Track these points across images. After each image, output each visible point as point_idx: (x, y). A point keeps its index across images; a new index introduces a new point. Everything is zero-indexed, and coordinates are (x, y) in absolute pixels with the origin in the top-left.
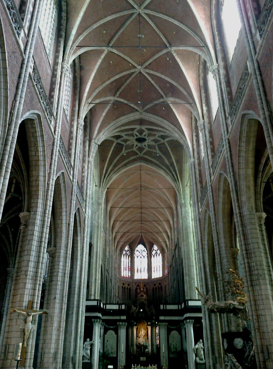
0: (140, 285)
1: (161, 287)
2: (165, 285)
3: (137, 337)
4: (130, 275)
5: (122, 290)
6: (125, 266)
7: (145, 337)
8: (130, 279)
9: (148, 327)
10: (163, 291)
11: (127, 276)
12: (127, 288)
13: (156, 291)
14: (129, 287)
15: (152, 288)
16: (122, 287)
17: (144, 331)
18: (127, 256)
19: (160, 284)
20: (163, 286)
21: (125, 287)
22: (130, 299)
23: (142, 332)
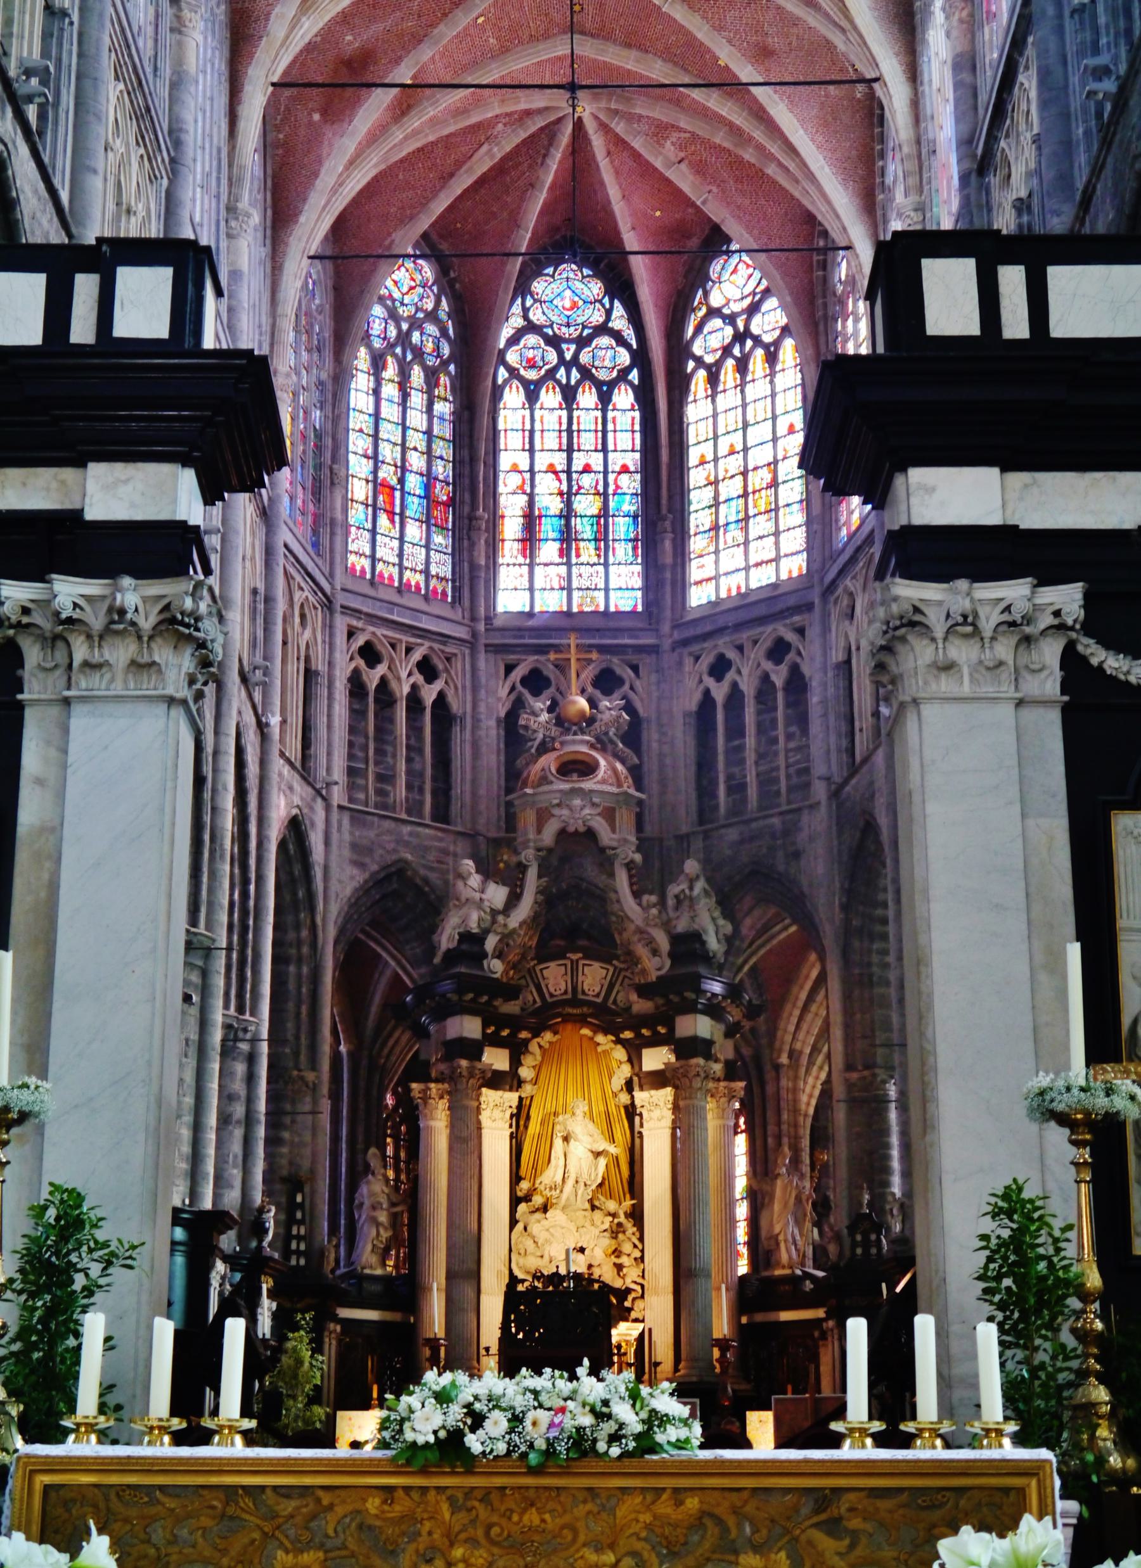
0: (549, 671)
1: (797, 684)
2: (837, 656)
3: (515, 1201)
4: (442, 566)
5: (357, 714)
6: (387, 473)
7: (612, 1206)
8: (447, 612)
9: (640, 1097)
10: (815, 726)
12: (414, 701)
13: (736, 730)
14: (429, 694)
15: (697, 696)
16: (356, 686)
17: (603, 1145)
18: (417, 376)
19: (778, 651)
20: (806, 669)
21: (383, 681)
22: (442, 814)
23: (579, 1151)
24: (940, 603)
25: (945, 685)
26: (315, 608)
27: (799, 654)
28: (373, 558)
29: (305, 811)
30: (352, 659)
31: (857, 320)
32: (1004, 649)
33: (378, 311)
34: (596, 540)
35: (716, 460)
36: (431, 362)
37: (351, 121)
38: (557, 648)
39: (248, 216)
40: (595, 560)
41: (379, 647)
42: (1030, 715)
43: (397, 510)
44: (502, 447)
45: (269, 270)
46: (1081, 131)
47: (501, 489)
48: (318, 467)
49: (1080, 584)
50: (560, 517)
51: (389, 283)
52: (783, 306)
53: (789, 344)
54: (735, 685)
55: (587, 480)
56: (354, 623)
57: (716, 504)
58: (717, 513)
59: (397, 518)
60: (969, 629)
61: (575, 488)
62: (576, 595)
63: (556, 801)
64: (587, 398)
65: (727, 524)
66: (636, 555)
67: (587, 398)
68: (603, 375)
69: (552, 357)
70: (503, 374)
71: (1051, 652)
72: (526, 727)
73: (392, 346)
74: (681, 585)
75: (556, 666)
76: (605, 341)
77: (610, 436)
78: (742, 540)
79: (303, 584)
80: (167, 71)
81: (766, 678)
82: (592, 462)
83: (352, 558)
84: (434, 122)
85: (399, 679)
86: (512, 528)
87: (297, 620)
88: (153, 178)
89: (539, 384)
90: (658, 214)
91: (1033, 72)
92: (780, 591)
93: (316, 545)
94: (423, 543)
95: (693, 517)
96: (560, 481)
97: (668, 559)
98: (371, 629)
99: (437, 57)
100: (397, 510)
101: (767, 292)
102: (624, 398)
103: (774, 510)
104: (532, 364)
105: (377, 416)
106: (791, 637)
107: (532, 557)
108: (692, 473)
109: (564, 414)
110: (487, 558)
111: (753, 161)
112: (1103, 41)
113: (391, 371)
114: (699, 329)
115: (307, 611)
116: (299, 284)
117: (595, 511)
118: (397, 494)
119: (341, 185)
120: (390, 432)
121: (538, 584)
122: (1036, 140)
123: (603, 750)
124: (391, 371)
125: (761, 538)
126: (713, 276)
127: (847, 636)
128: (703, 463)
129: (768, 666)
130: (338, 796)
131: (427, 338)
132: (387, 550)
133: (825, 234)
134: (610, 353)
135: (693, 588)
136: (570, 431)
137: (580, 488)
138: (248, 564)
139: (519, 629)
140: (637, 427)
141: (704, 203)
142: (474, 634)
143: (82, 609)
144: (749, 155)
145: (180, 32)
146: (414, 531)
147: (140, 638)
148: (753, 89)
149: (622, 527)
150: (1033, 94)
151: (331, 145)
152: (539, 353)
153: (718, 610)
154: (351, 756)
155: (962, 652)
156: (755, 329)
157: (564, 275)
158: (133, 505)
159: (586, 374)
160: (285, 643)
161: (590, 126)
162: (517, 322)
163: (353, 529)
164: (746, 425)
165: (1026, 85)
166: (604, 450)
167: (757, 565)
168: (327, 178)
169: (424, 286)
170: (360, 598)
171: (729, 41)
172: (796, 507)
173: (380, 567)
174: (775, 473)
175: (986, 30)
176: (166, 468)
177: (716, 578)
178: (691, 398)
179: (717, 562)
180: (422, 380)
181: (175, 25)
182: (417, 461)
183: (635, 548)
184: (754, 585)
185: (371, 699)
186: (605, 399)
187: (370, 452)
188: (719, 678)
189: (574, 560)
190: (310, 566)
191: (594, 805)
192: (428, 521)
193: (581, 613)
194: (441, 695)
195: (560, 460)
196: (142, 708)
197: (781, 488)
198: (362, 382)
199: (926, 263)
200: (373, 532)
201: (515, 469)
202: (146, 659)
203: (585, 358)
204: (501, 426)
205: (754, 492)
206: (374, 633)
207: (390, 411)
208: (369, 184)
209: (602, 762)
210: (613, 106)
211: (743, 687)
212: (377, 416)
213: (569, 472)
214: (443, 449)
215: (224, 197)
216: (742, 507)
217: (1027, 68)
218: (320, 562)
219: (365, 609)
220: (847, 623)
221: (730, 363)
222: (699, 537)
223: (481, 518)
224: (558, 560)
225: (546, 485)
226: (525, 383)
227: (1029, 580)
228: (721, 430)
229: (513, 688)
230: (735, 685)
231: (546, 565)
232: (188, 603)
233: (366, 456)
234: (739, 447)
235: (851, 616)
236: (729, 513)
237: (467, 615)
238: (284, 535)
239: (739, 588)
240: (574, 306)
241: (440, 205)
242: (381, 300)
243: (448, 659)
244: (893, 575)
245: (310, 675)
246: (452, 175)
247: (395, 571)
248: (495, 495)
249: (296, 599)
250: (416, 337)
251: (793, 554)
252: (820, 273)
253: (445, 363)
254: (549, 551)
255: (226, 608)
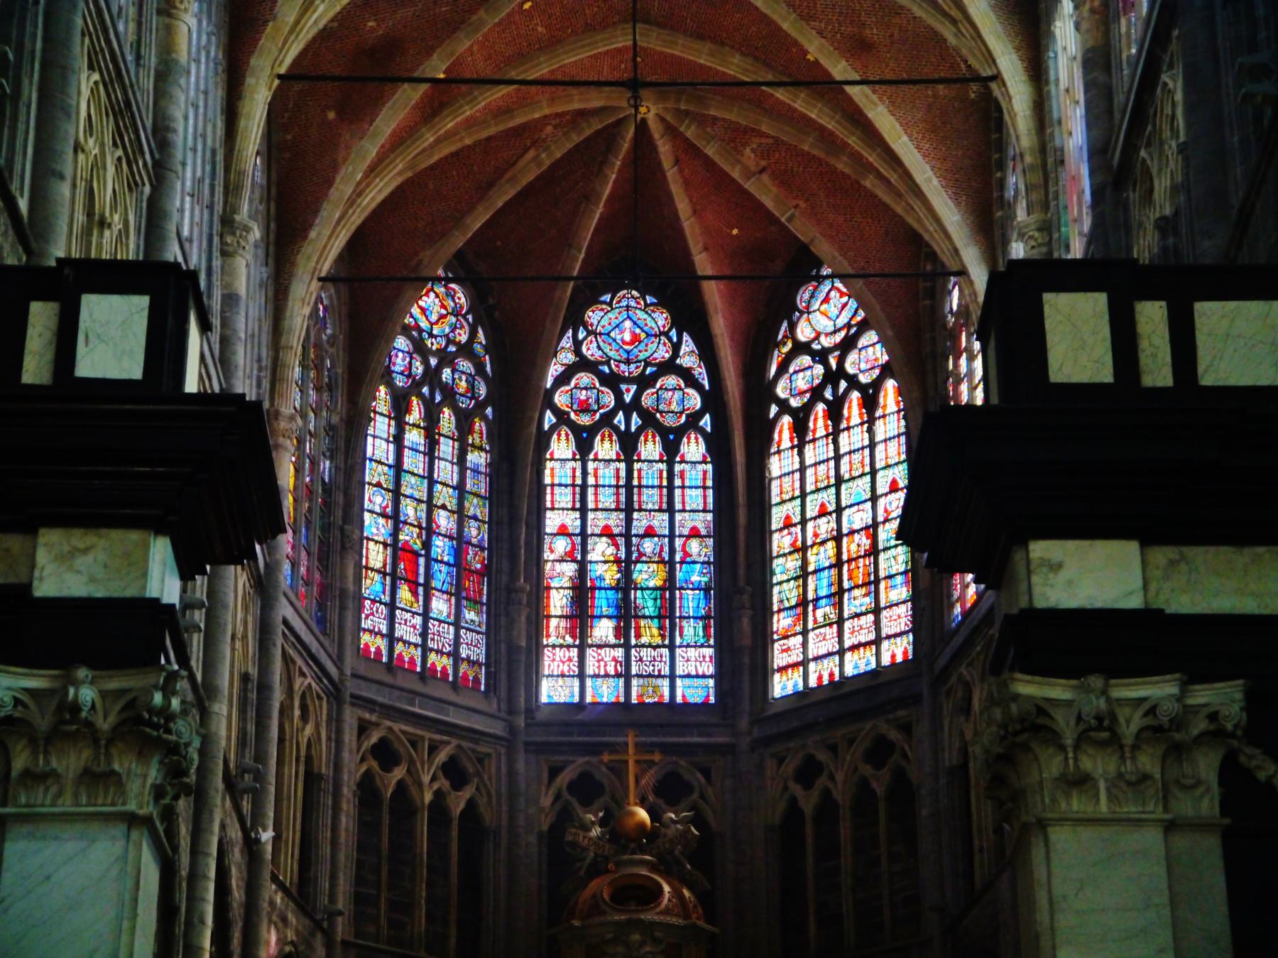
0: (602, 775)
2: (950, 758)
4: (473, 648)
5: (367, 826)
11: (441, 662)
14: (458, 802)
15: (782, 806)
18: (447, 420)
19: (879, 751)
24: (1069, 703)
25: (1077, 804)
26: (319, 698)
27: (905, 756)
28: (391, 638)
29: (301, 948)
30: (363, 760)
31: (971, 358)
32: (1148, 762)
33: (401, 342)
34: (659, 617)
35: (804, 522)
36: (464, 403)
37: (372, 121)
38: (612, 748)
39: (247, 229)
40: (658, 640)
41: (396, 745)
42: (1181, 842)
43: (421, 580)
44: (549, 505)
45: (270, 294)
46: (1236, 139)
47: (547, 555)
48: (326, 528)
49: (1240, 682)
50: (615, 588)
51: (415, 310)
52: (883, 340)
53: (890, 384)
54: (827, 793)
55: (648, 546)
56: (367, 716)
57: (804, 574)
58: (805, 586)
59: (421, 590)
60: (1105, 735)
61: (634, 556)
62: (634, 682)
63: (609, 936)
64: (650, 448)
65: (817, 599)
66: (707, 636)
67: (650, 448)
68: (669, 421)
69: (609, 399)
70: (549, 418)
71: (1206, 765)
72: (574, 844)
73: (416, 385)
74: (763, 672)
75: (608, 768)
76: (672, 380)
77: (678, 492)
78: (834, 617)
79: (305, 669)
80: (152, 60)
81: (864, 784)
82: (655, 523)
83: (365, 638)
84: (470, 124)
85: (420, 785)
86: (558, 602)
87: (297, 713)
88: (133, 186)
89: (593, 430)
90: (735, 232)
91: (1179, 70)
92: (881, 680)
93: (322, 621)
94: (452, 619)
95: (776, 590)
96: (617, 546)
97: (747, 642)
98: (388, 723)
99: (475, 48)
100: (421, 580)
101: (864, 326)
102: (693, 448)
103: (873, 583)
104: (584, 408)
105: (398, 467)
106: (894, 735)
107: (583, 636)
108: (776, 536)
109: (622, 466)
110: (529, 638)
111: (847, 171)
112: (1262, 35)
113: (415, 416)
114: (783, 368)
115: (309, 701)
116: (307, 311)
117: (656, 582)
118: (422, 561)
119: (359, 195)
120: (413, 486)
121: (590, 670)
122: (1182, 149)
123: (667, 875)
124: (415, 416)
125: (858, 615)
126: (802, 306)
127: (962, 734)
128: (788, 524)
129: (867, 770)
130: (341, 928)
131: (459, 376)
132: (407, 629)
133: (933, 256)
134: (678, 394)
135: (777, 677)
136: (629, 487)
137: (641, 554)
138: (238, 644)
139: (567, 724)
140: (709, 483)
141: (790, 220)
142: (512, 730)
143: (25, 706)
144: (842, 165)
145: (170, 15)
146: (440, 606)
147: (96, 741)
148: (848, 89)
149: (691, 602)
150: (1179, 96)
151: (348, 147)
152: (593, 394)
153: (807, 701)
154: (359, 880)
155: (1098, 764)
156: (850, 368)
157: (624, 303)
158: (93, 580)
159: (649, 419)
160: (281, 740)
161: (655, 128)
162: (567, 357)
163: (367, 603)
164: (839, 481)
165: (1171, 85)
166: (671, 510)
167: (854, 648)
168: (342, 188)
169: (456, 313)
170: (374, 687)
171: (820, 33)
172: (899, 580)
173: (399, 648)
174: (874, 538)
175: (1123, 21)
176: (134, 536)
177: (804, 663)
178: (774, 449)
179: (805, 644)
180: (453, 426)
181: (163, 5)
182: (444, 521)
183: (706, 628)
184: (849, 671)
185: (386, 809)
186: (671, 451)
187: (389, 510)
188: (808, 785)
189: (633, 641)
190: (314, 646)
191: (655, 941)
192: (458, 594)
193: (642, 704)
194: (471, 804)
195: (616, 521)
196: (95, 827)
197: (882, 556)
198: (382, 426)
199: (1048, 297)
200: (392, 606)
201: (563, 531)
202: (103, 767)
203: (648, 400)
204: (547, 480)
205: (850, 561)
206: (390, 729)
207: (415, 462)
208: (392, 194)
209: (667, 888)
210: (683, 107)
211: (837, 796)
212: (398, 467)
213: (627, 536)
214: (475, 507)
215: (219, 208)
216: (835, 579)
217: (1171, 66)
218: (327, 643)
219: (380, 699)
220: (962, 719)
221: (820, 407)
222: (782, 615)
223: (521, 590)
224: (612, 640)
225: (600, 549)
226: (576, 429)
227: (1177, 676)
228: (809, 488)
229: (558, 797)
230: (827, 793)
231: (600, 647)
232: (158, 698)
233: (383, 515)
234: (831, 508)
235: (966, 709)
236: (820, 585)
237: (503, 706)
238: (285, 610)
239: (831, 675)
240: (635, 339)
241: (477, 221)
242: (406, 331)
243: (480, 761)
244: (1012, 669)
245: (312, 779)
246: (491, 185)
247: (417, 653)
248: (539, 562)
249: (296, 687)
250: (446, 374)
251: (896, 635)
252: (927, 302)
253: (481, 406)
254: (604, 630)
255: (209, 698)
